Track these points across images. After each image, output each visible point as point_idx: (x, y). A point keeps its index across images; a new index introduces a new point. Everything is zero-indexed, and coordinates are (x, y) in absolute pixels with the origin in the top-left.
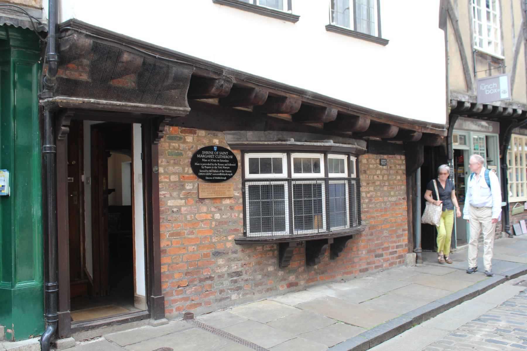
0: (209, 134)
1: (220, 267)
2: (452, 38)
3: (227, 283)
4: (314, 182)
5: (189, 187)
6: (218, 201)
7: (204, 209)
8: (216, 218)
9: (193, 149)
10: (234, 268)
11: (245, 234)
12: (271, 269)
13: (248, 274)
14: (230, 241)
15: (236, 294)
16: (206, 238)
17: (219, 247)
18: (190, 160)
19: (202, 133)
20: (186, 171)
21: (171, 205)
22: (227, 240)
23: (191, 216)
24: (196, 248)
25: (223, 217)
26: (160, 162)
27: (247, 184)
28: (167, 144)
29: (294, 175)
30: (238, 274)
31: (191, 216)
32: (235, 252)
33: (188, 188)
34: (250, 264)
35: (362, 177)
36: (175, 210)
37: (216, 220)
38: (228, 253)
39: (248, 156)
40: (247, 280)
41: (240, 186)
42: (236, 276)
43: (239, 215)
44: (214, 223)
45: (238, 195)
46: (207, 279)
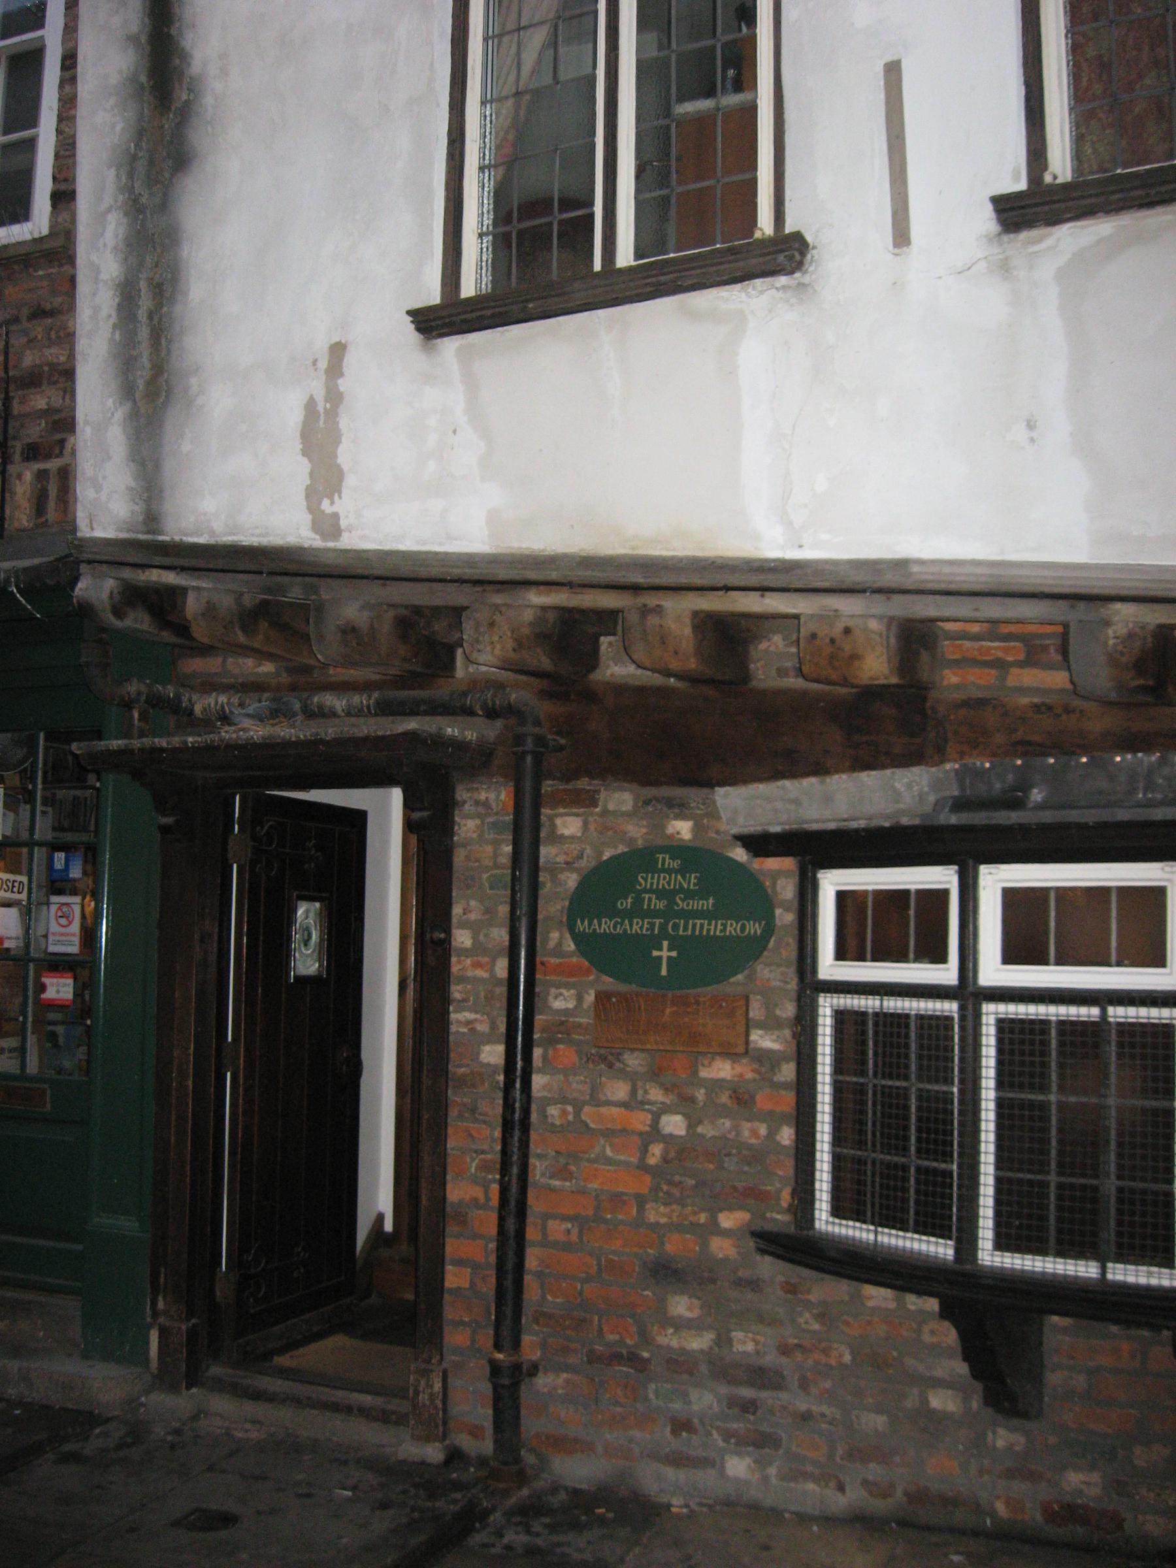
0: (647, 803)
1: (679, 1325)
7: (619, 1090)
9: (583, 863)
13: (814, 1391)
15: (748, 1460)
16: (617, 1200)
18: (567, 903)
19: (620, 799)
22: (713, 1228)
23: (564, 1113)
24: (575, 1231)
25: (700, 1129)
26: (457, 910)
27: (826, 1006)
28: (489, 849)
33: (558, 1004)
37: (668, 1139)
39: (832, 883)
40: (806, 1417)
41: (789, 1010)
42: (751, 1384)
43: (772, 1133)
44: (656, 1150)
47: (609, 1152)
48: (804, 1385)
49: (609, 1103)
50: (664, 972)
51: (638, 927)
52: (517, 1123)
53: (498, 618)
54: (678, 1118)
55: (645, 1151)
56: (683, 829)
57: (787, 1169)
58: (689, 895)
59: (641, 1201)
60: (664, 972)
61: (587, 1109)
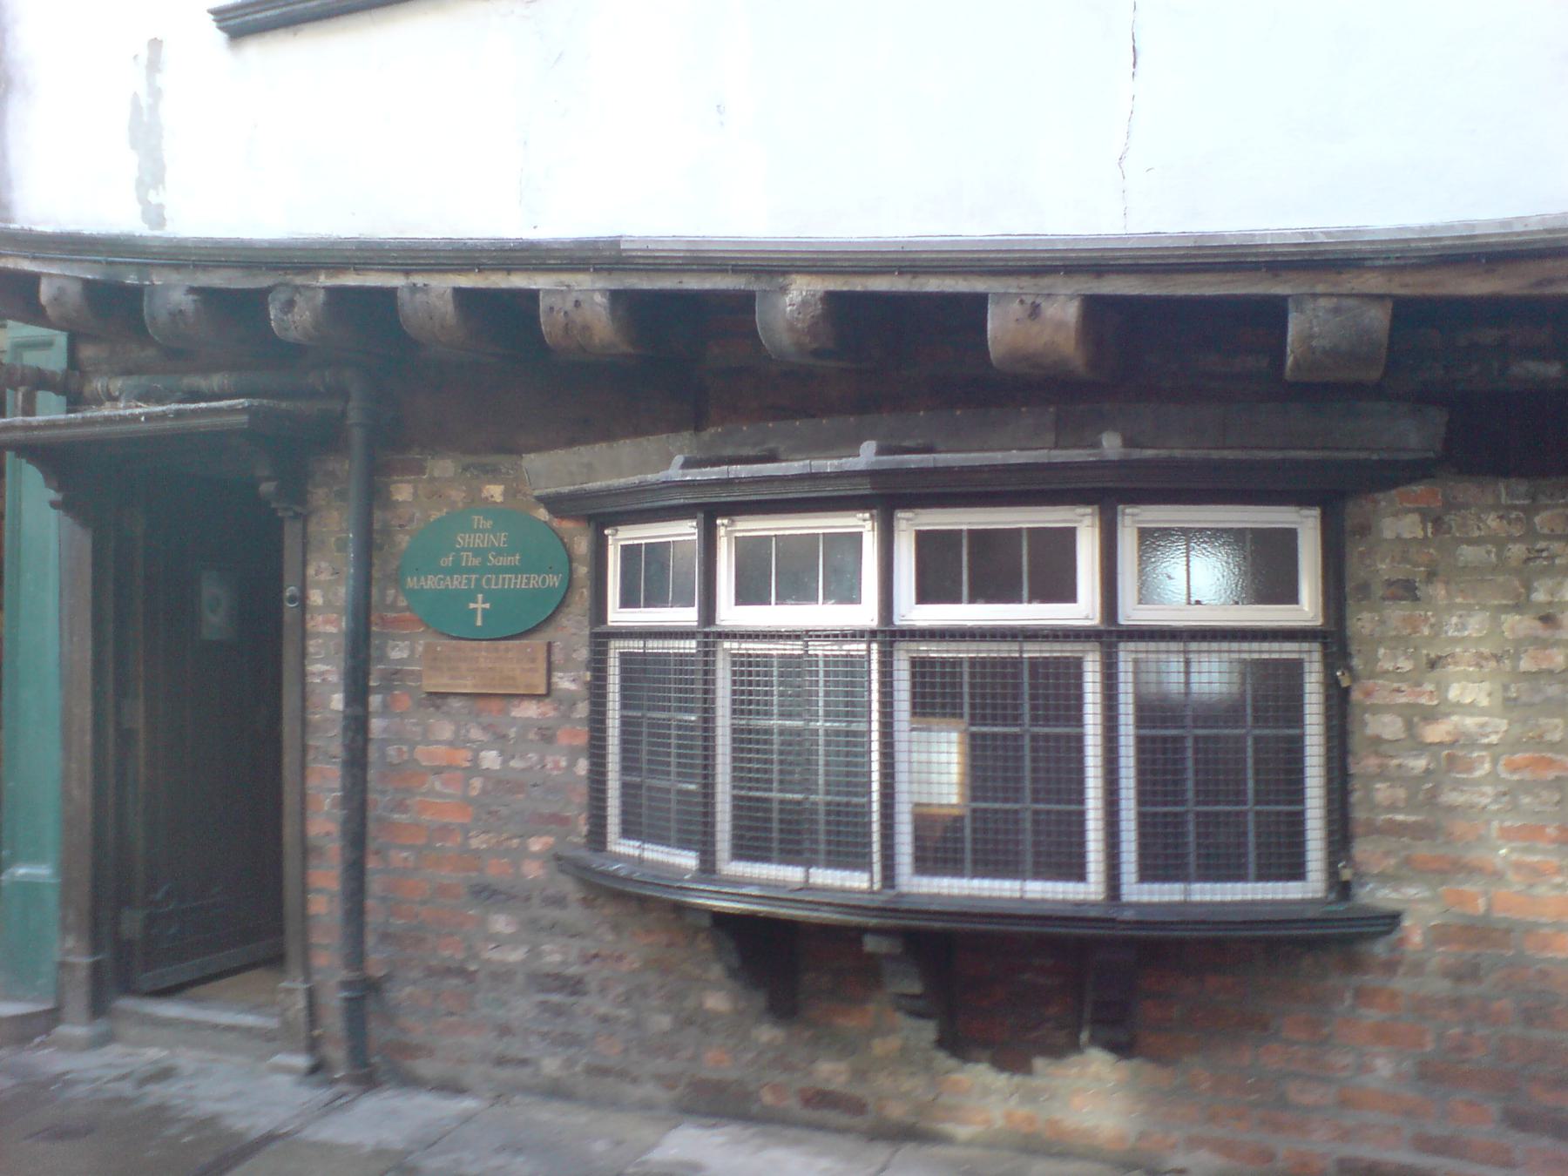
0: (465, 469)
1: (500, 941)
3: (522, 1007)
4: (793, 648)
6: (495, 705)
7: (446, 731)
8: (485, 765)
10: (553, 956)
11: (597, 836)
12: (717, 1002)
14: (535, 856)
16: (445, 831)
17: (495, 871)
20: (389, 600)
22: (523, 852)
25: (513, 764)
27: (616, 648)
30: (574, 986)
31: (400, 750)
32: (558, 901)
34: (620, 958)
35: (1362, 622)
37: (487, 774)
38: (528, 899)
40: (604, 1019)
41: (583, 654)
43: (572, 764)
44: (477, 783)
45: (573, 687)
46: (448, 971)
48: (603, 990)
49: (438, 742)
50: (479, 623)
51: (458, 582)
52: (357, 760)
53: (297, 297)
54: (494, 753)
55: (467, 785)
56: (495, 491)
57: (580, 796)
58: (500, 553)
59: (466, 830)
60: (479, 623)
61: (420, 748)
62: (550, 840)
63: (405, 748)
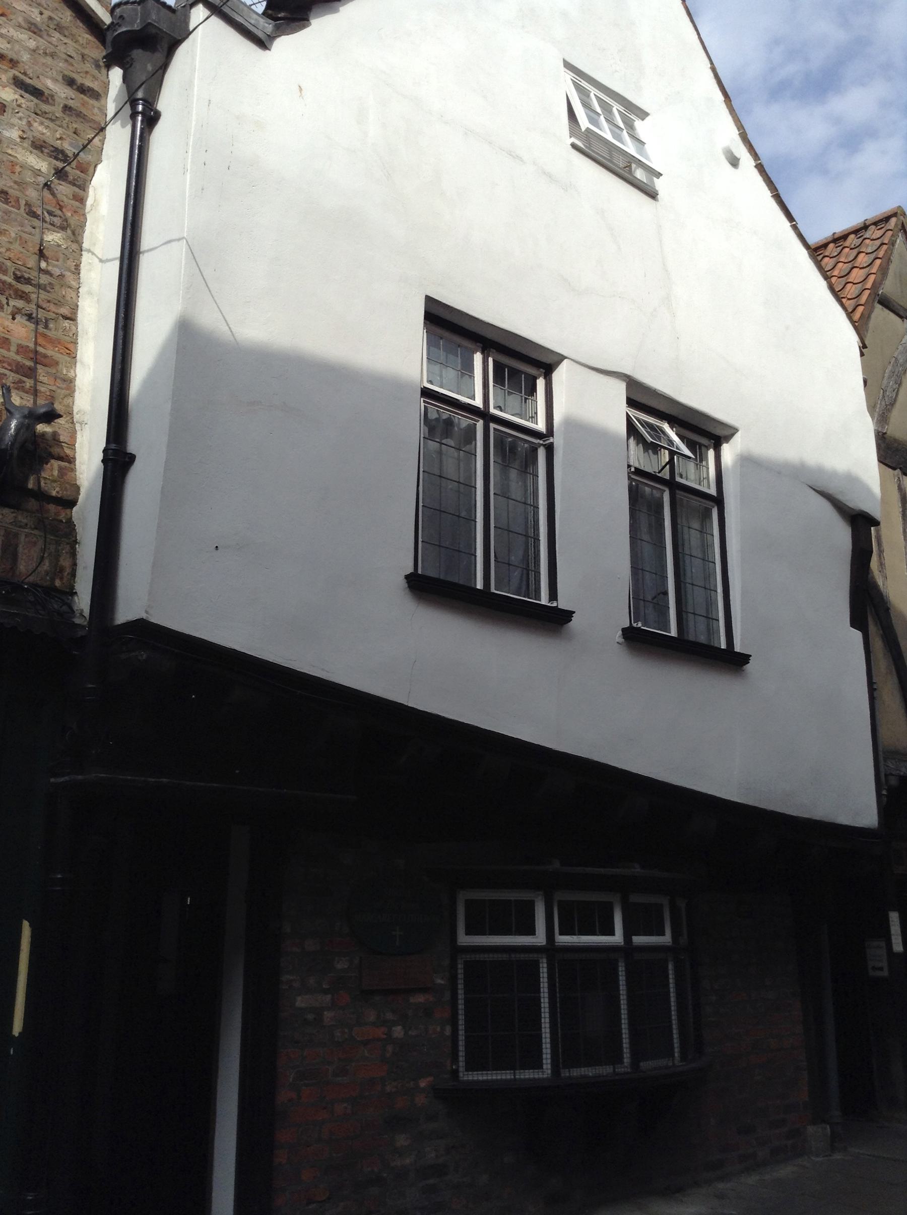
2: (878, 644)
5: (341, 965)
11: (455, 1073)
21: (303, 1005)
25: (410, 1033)
29: (563, 940)
33: (339, 966)
36: (310, 1017)
44: (390, 1048)
47: (367, 1054)
54: (399, 1028)
62: (431, 1079)
63: (346, 1030)
